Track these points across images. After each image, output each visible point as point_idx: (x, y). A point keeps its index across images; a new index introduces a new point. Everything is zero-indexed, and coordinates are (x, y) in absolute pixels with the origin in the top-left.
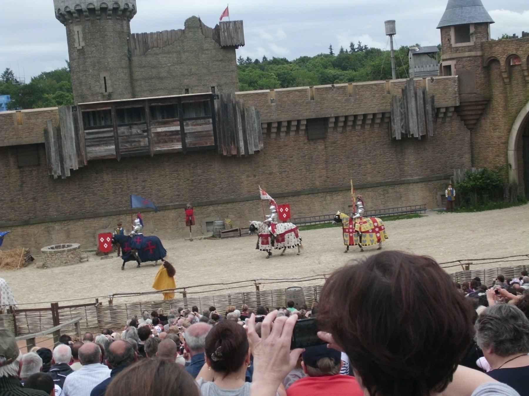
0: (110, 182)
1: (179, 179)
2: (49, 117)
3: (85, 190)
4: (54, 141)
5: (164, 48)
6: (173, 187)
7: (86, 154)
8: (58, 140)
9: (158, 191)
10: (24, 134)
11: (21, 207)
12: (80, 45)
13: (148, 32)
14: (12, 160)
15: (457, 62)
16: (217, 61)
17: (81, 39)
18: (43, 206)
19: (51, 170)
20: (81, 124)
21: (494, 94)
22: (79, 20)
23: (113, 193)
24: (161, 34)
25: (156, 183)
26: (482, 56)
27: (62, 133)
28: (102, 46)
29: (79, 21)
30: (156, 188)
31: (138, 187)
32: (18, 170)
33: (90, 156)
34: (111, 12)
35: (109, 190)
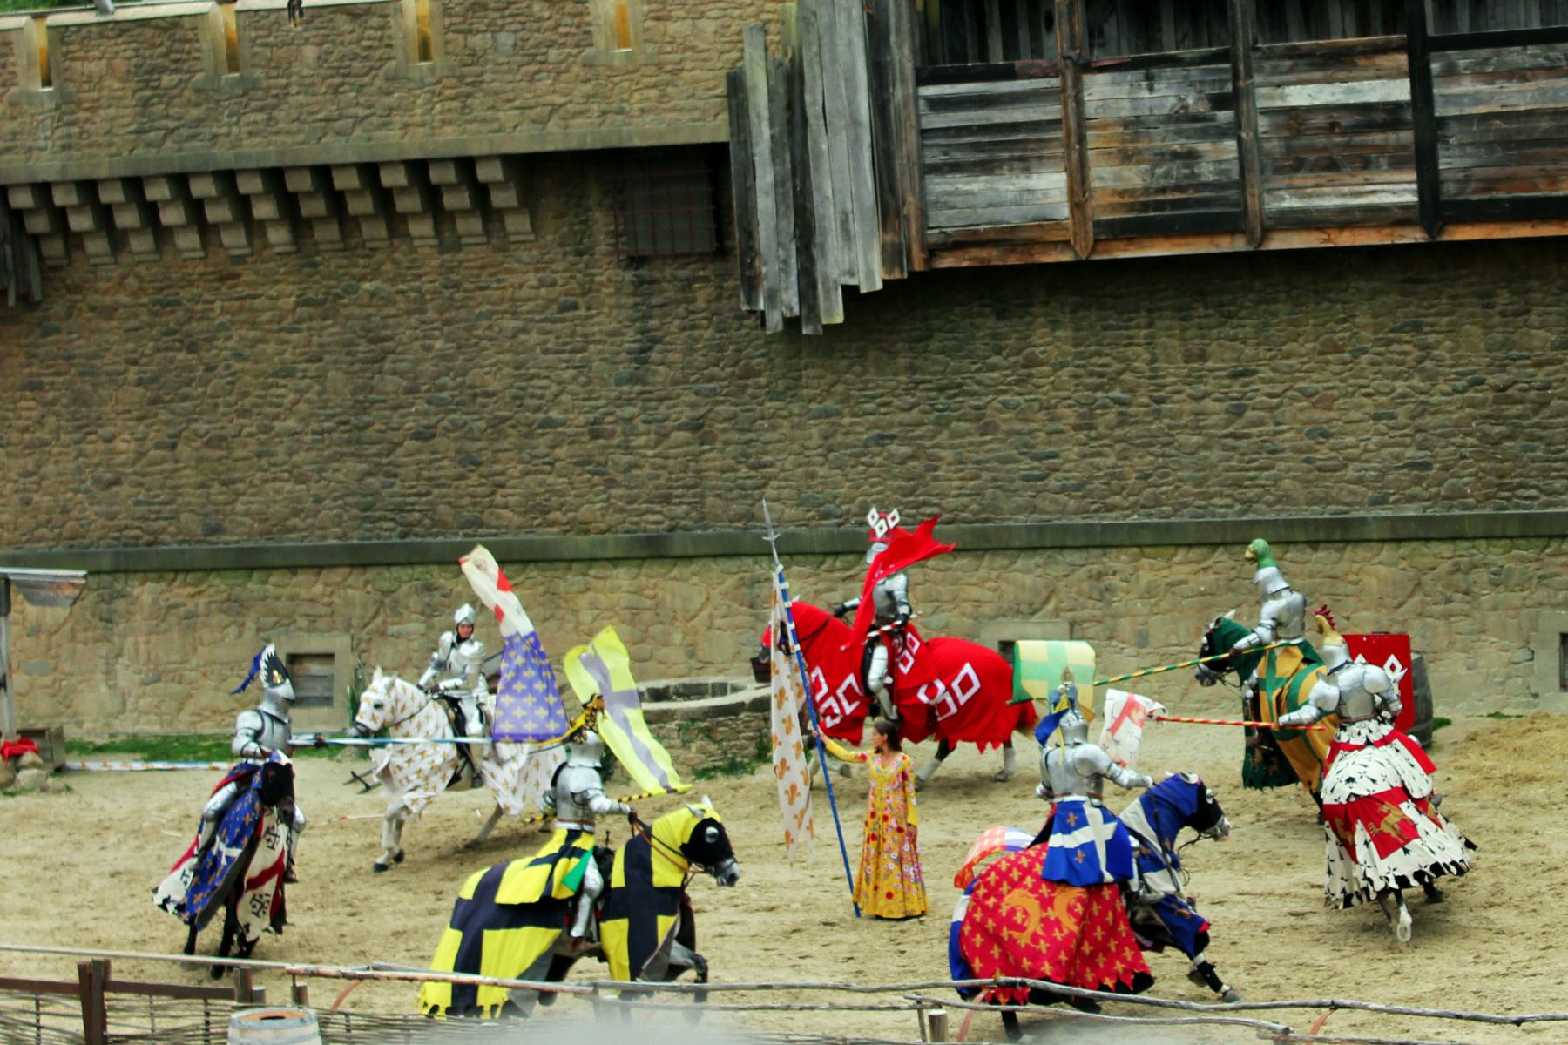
0: (1063, 365)
1: (1431, 378)
2: (750, 10)
3: (942, 401)
4: (772, 137)
6: (1392, 417)
7: (923, 215)
8: (791, 134)
9: (1308, 434)
10: (637, 96)
11: (636, 466)
14: (601, 221)
18: (735, 470)
19: (751, 284)
20: (902, 55)
23: (1076, 428)
25: (1300, 390)
27: (807, 98)
30: (1302, 416)
31: (1208, 404)
32: (629, 275)
33: (944, 220)
35: (1061, 411)
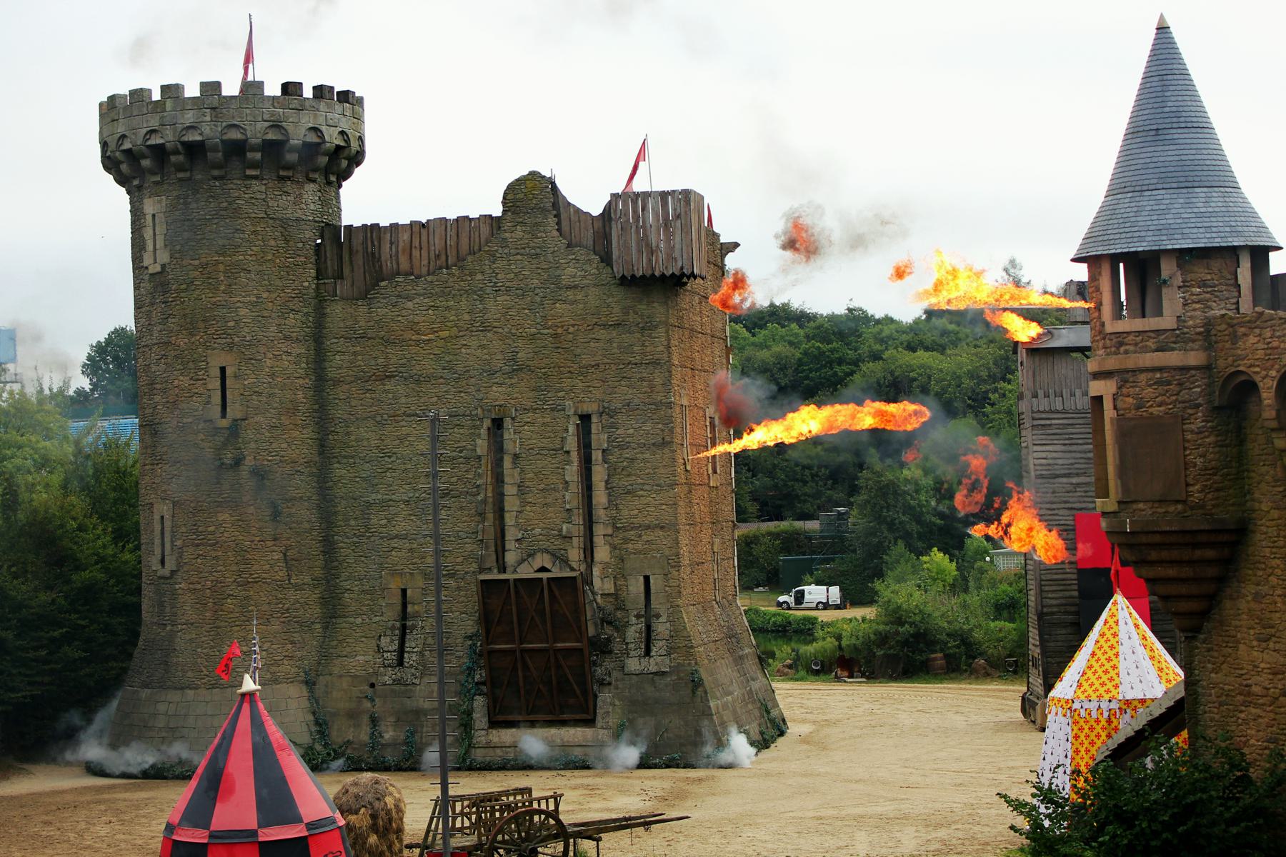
5: (429, 278)
12: (155, 262)
13: (384, 223)
15: (1119, 388)
16: (605, 326)
17: (160, 243)
21: (1257, 505)
22: (158, 178)
24: (424, 232)
26: (1207, 368)
28: (221, 267)
29: (156, 183)
34: (258, 156)
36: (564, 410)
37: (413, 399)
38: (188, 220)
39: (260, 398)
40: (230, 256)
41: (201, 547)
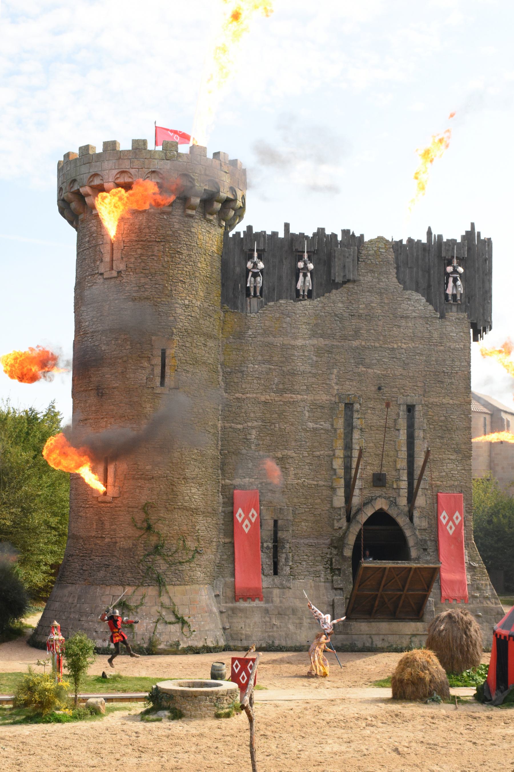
12: (112, 269)
36: (397, 401)
37: (289, 386)
38: (142, 241)
39: (188, 375)
40: (171, 270)
41: (140, 481)
